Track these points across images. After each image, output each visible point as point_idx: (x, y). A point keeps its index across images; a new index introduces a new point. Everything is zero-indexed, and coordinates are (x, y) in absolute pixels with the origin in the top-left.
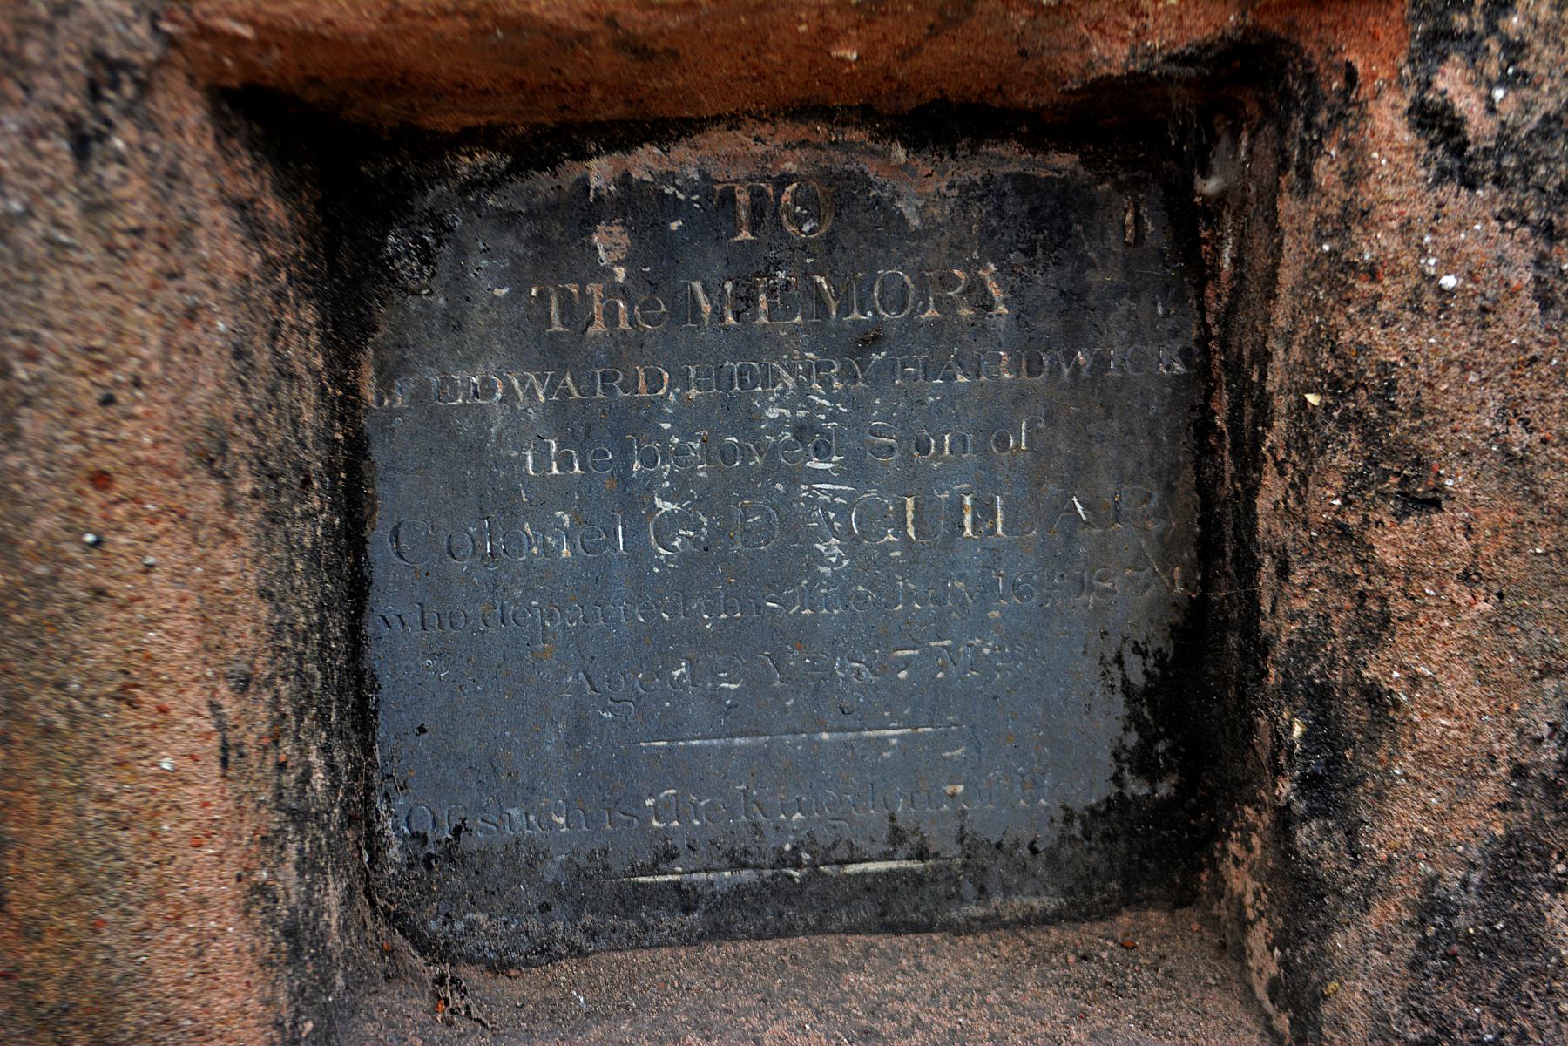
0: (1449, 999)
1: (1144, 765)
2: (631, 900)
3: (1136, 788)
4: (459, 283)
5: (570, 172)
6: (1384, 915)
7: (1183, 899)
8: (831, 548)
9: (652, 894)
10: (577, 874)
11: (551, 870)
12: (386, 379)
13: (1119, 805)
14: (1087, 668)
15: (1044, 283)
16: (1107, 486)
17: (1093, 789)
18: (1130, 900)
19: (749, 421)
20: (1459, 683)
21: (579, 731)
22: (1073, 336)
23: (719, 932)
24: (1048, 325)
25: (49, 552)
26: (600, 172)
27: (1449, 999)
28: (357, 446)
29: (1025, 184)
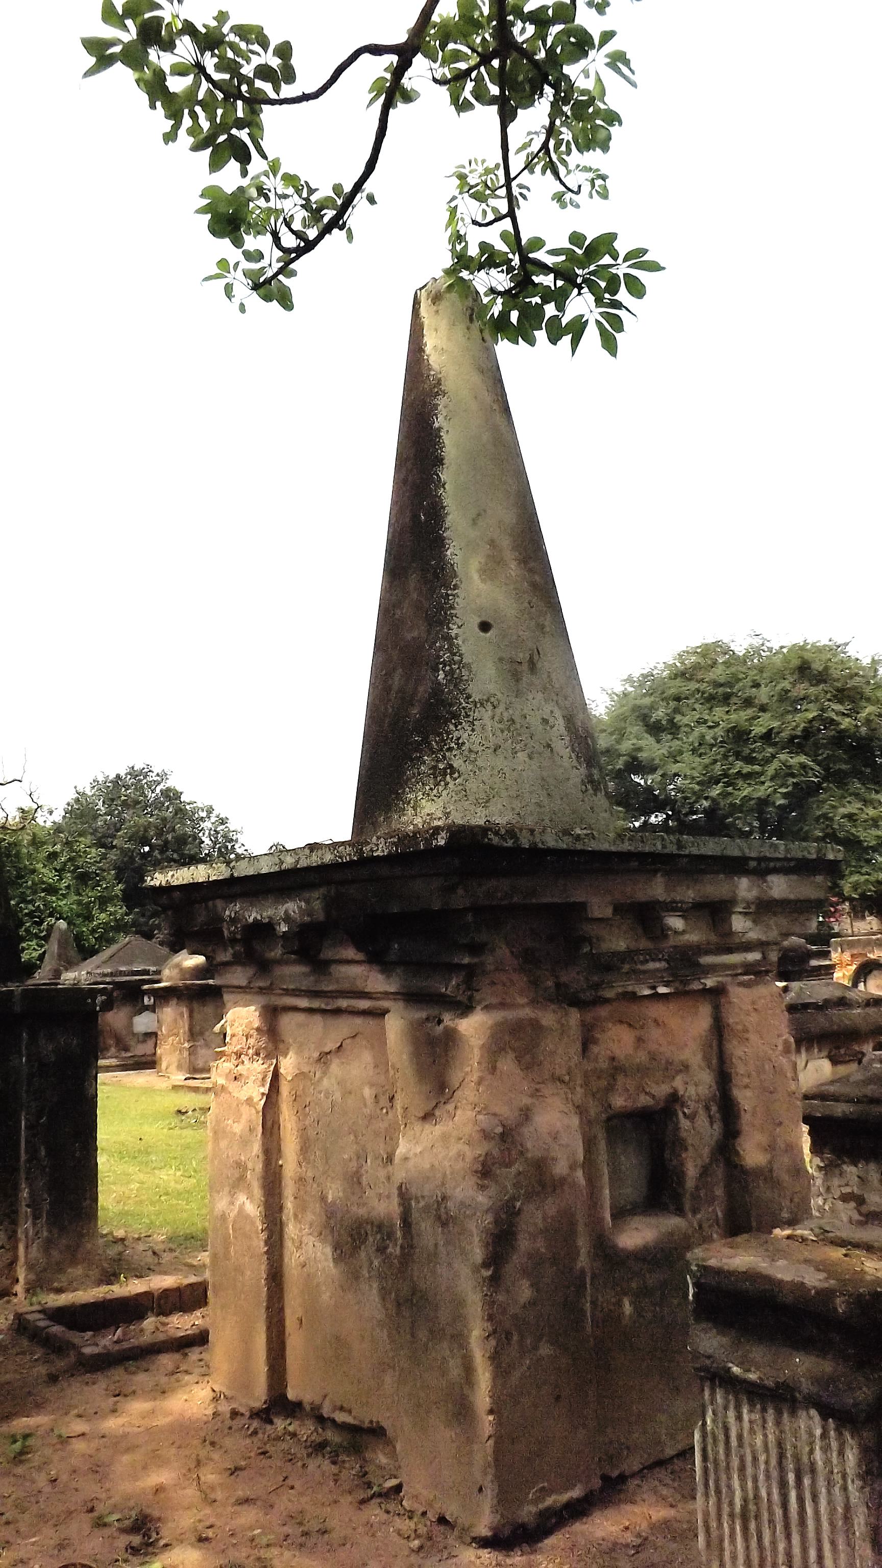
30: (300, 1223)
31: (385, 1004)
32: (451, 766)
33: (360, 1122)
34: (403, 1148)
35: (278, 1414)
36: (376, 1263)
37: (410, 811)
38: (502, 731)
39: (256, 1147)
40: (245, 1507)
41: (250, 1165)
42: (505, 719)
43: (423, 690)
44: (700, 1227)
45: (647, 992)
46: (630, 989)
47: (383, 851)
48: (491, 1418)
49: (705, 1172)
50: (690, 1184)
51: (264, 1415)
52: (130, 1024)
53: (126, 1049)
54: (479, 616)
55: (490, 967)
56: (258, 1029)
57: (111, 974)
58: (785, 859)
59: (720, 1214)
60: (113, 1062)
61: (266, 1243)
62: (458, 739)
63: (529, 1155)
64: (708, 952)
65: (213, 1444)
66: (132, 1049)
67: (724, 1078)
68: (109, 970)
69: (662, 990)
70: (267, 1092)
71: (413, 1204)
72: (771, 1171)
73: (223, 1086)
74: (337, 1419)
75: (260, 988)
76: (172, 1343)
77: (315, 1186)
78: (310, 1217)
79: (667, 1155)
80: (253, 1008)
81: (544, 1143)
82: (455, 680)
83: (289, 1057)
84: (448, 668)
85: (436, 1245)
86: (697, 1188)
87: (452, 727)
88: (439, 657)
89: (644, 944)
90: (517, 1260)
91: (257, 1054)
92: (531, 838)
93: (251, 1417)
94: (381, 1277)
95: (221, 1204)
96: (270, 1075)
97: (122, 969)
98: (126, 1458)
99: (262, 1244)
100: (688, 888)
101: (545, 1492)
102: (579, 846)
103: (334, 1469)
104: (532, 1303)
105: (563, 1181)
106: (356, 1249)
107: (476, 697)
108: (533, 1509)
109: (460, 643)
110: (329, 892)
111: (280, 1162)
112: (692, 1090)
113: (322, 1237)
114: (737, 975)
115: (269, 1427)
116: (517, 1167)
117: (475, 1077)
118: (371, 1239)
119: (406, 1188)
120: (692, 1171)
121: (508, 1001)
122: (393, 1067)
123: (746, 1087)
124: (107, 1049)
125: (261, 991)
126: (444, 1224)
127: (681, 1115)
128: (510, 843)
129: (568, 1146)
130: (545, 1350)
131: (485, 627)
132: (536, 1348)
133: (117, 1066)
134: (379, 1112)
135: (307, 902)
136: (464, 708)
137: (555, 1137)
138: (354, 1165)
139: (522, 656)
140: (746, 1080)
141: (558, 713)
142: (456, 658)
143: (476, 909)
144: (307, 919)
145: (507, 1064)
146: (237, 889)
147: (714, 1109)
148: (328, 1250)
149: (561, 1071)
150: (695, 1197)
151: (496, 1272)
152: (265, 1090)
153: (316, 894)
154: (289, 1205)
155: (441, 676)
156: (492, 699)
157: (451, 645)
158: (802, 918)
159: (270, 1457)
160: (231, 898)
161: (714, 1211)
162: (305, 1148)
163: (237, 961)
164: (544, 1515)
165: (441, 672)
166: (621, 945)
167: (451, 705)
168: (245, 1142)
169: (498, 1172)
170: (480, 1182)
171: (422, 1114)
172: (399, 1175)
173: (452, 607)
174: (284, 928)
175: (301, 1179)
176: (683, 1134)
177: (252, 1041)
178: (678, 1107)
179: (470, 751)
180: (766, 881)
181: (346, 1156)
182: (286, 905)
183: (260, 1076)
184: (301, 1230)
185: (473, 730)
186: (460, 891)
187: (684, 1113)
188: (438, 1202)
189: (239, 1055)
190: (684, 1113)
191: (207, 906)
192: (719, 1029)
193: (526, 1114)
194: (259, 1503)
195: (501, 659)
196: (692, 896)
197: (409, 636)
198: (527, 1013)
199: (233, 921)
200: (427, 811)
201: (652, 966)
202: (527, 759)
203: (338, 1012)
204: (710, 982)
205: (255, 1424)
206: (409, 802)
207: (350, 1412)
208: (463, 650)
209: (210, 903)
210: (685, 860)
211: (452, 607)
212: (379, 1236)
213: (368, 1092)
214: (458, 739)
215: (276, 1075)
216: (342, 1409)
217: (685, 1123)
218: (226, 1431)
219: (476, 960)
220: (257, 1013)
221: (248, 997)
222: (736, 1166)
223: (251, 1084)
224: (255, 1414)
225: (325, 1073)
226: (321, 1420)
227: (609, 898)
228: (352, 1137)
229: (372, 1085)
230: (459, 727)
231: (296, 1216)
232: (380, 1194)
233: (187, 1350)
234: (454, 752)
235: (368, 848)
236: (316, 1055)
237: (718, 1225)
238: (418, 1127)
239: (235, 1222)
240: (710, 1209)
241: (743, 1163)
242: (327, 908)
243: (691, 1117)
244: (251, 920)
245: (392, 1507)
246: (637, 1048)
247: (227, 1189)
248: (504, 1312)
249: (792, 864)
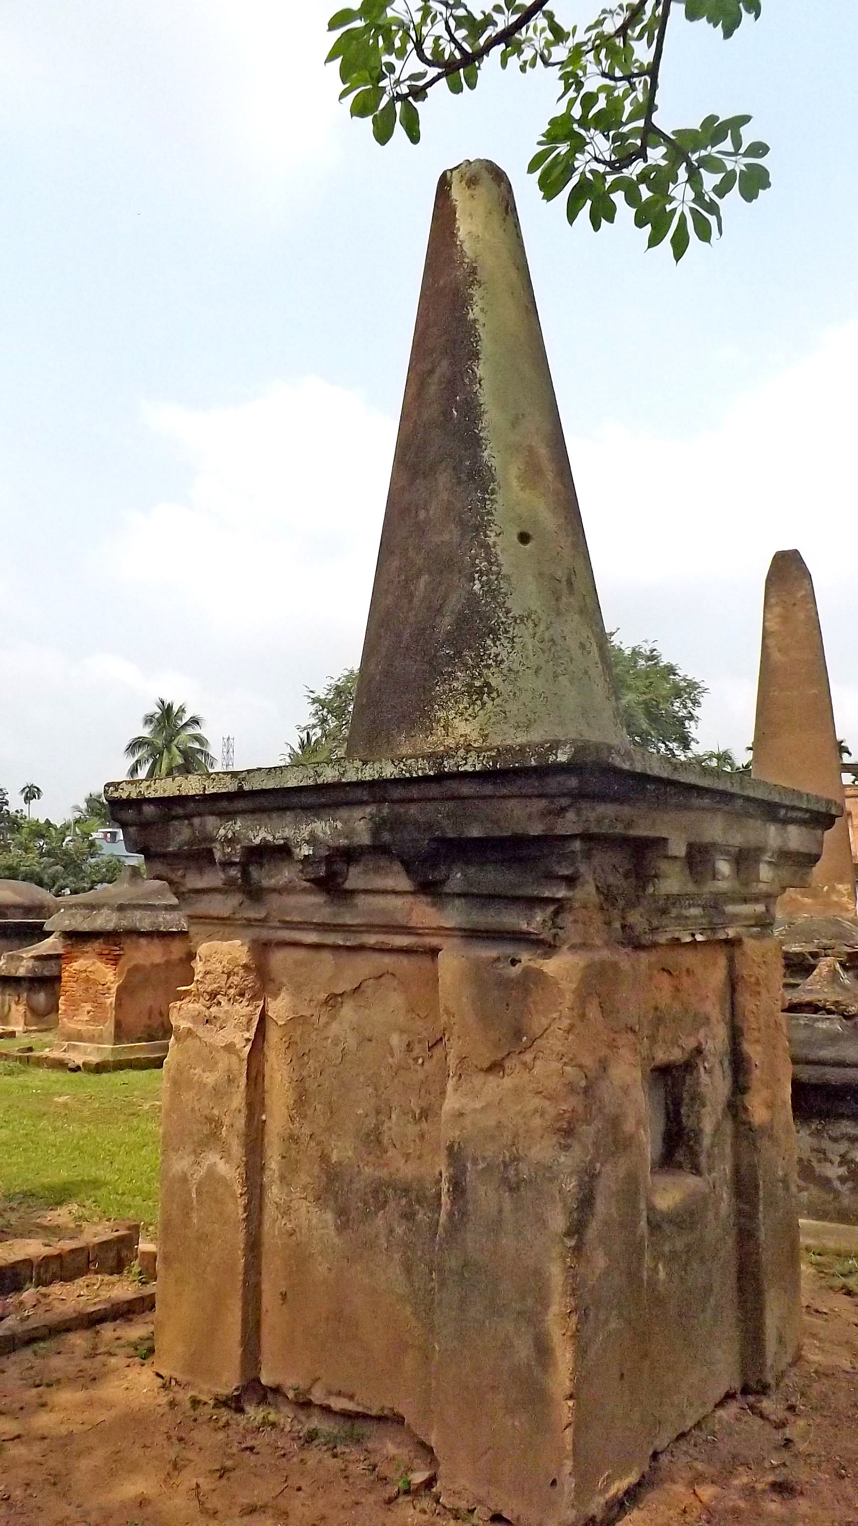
30: (289, 1185)
31: (434, 941)
32: (487, 684)
33: (384, 1073)
34: (451, 1103)
35: (250, 1402)
36: (399, 1231)
37: (440, 731)
38: (543, 651)
39: (238, 1100)
40: (256, 1516)
41: (227, 1121)
42: (546, 639)
43: (455, 602)
45: (688, 939)
46: (677, 935)
47: (475, 766)
48: (570, 1403)
49: (717, 1131)
50: (706, 1141)
51: (235, 1404)
55: (577, 905)
56: (245, 967)
58: (807, 810)
61: (246, 1208)
62: (497, 655)
63: (606, 1111)
65: (181, 1440)
67: (736, 1035)
69: (699, 938)
70: (252, 1038)
71: (469, 1165)
72: (772, 1128)
73: (189, 1029)
74: (333, 1405)
75: (248, 920)
76: (82, 1320)
77: (313, 1144)
78: (304, 1179)
79: (683, 1110)
80: (238, 942)
82: (491, 592)
83: (280, 999)
84: (484, 578)
85: (500, 1211)
86: (712, 1146)
87: (489, 642)
88: (474, 565)
89: (691, 888)
90: (593, 1229)
91: (242, 995)
93: (215, 1406)
94: (407, 1246)
95: (181, 1164)
96: (256, 1019)
98: (85, 1464)
99: (241, 1210)
101: (610, 1480)
103: (338, 1463)
104: (606, 1273)
106: (367, 1216)
108: (602, 1500)
109: (499, 552)
110: (379, 811)
111: (264, 1117)
113: (321, 1201)
115: (239, 1417)
117: (566, 1023)
118: (392, 1204)
119: (460, 1148)
120: (708, 1126)
121: (590, 942)
122: (447, 1011)
123: (758, 1041)
125: (250, 923)
126: (513, 1189)
127: (702, 1069)
131: (524, 538)
132: (607, 1321)
134: (411, 1062)
135: (345, 822)
136: (502, 623)
138: (371, 1122)
142: (494, 568)
143: (587, 837)
144: (343, 842)
145: (593, 1012)
146: (240, 804)
147: (726, 1063)
148: (329, 1216)
149: (632, 1021)
151: (580, 1240)
152: (251, 1035)
153: (358, 813)
154: (273, 1163)
155: (477, 586)
156: (533, 617)
157: (488, 553)
159: (258, 1453)
160: (227, 815)
161: (724, 1169)
162: (302, 1099)
163: (228, 888)
164: (609, 1506)
165: (477, 582)
167: (489, 619)
168: (218, 1093)
169: (580, 1129)
170: (562, 1141)
171: (486, 1065)
172: (449, 1133)
173: (489, 513)
174: (306, 850)
175: (291, 1137)
176: (703, 1089)
177: (235, 980)
178: (699, 1061)
179: (510, 670)
180: (786, 832)
181: (360, 1111)
182: (314, 825)
183: (244, 1020)
184: (289, 1193)
185: (513, 648)
186: (571, 815)
187: (705, 1068)
188: (504, 1162)
189: (213, 995)
191: (191, 825)
192: (733, 983)
193: (604, 1065)
194: (270, 1511)
195: (541, 574)
196: (740, 840)
197: (436, 539)
198: (605, 954)
199: (230, 841)
200: (462, 731)
201: (694, 911)
203: (361, 948)
204: (731, 933)
205: (225, 1415)
206: (439, 721)
207: (351, 1397)
208: (502, 559)
209: (196, 821)
211: (489, 513)
212: (404, 1202)
213: (395, 1040)
214: (497, 655)
215: (263, 1017)
216: (339, 1394)
217: (704, 1078)
218: (192, 1424)
219: (569, 894)
220: (246, 948)
221: (227, 930)
222: (744, 1123)
223: (230, 1026)
224: (221, 1403)
225: (333, 1018)
226: (305, 1405)
228: (371, 1090)
229: (402, 1031)
230: (498, 643)
231: (282, 1178)
232: (409, 1154)
233: (98, 1327)
234: (493, 670)
235: (452, 762)
236: (323, 996)
238: (478, 1080)
239: (200, 1185)
241: (751, 1120)
242: (376, 832)
244: (257, 841)
245: (426, 1503)
246: (674, 998)
247: (189, 1147)
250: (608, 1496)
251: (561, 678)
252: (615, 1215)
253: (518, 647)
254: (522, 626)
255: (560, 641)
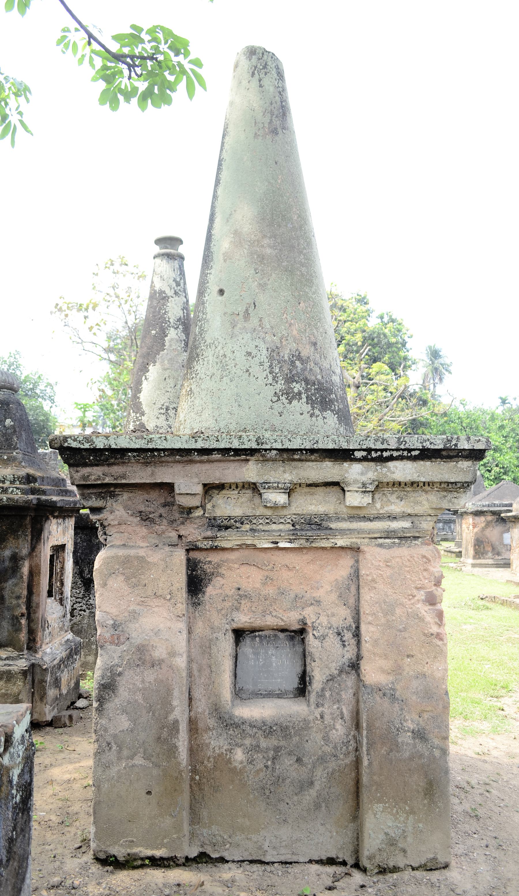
0: (319, 700)
1: (300, 684)
2: (257, 694)
3: (300, 686)
4: (246, 642)
5: (255, 633)
6: (314, 693)
7: (304, 696)
8: (274, 664)
9: (258, 694)
10: (252, 692)
11: (250, 691)
12: (239, 649)
13: (298, 687)
14: (295, 675)
15: (291, 643)
16: (297, 660)
17: (296, 686)
18: (299, 696)
19: (268, 653)
20: (318, 675)
21: (253, 679)
22: (294, 647)
23: (264, 697)
24: (292, 646)
25: (220, 661)
26: (257, 634)
27: (319, 700)
28: (237, 654)
29: (290, 635)
38: (217, 364)
44: (322, 717)
52: (501, 538)
53: (498, 554)
54: (219, 286)
57: (489, 506)
58: (397, 450)
59: (344, 711)
60: (490, 562)
64: (338, 519)
66: (503, 554)
68: (487, 503)
69: (281, 545)
81: (146, 635)
86: (323, 690)
92: (106, 442)
97: (495, 502)
100: (284, 472)
102: (150, 446)
105: (161, 662)
107: (209, 341)
112: (324, 620)
114: (376, 538)
116: (124, 647)
124: (486, 553)
127: (311, 634)
128: (87, 446)
129: (167, 640)
130: (139, 761)
131: (221, 292)
132: (132, 757)
133: (493, 564)
137: (157, 633)
139: (241, 309)
140: (370, 618)
141: (263, 347)
150: (321, 695)
158: (450, 496)
166: (237, 512)
173: (208, 282)
179: (200, 379)
187: (313, 635)
190: (313, 635)
193: (134, 616)
202: (228, 381)
210: (274, 452)
227: (196, 480)
237: (342, 718)
240: (335, 707)
243: (323, 638)
246: (264, 584)
248: (106, 730)
249: (417, 453)
250: (129, 851)
251: (225, 378)
252: (141, 701)
253: (205, 363)
254: (210, 350)
255: (229, 354)
